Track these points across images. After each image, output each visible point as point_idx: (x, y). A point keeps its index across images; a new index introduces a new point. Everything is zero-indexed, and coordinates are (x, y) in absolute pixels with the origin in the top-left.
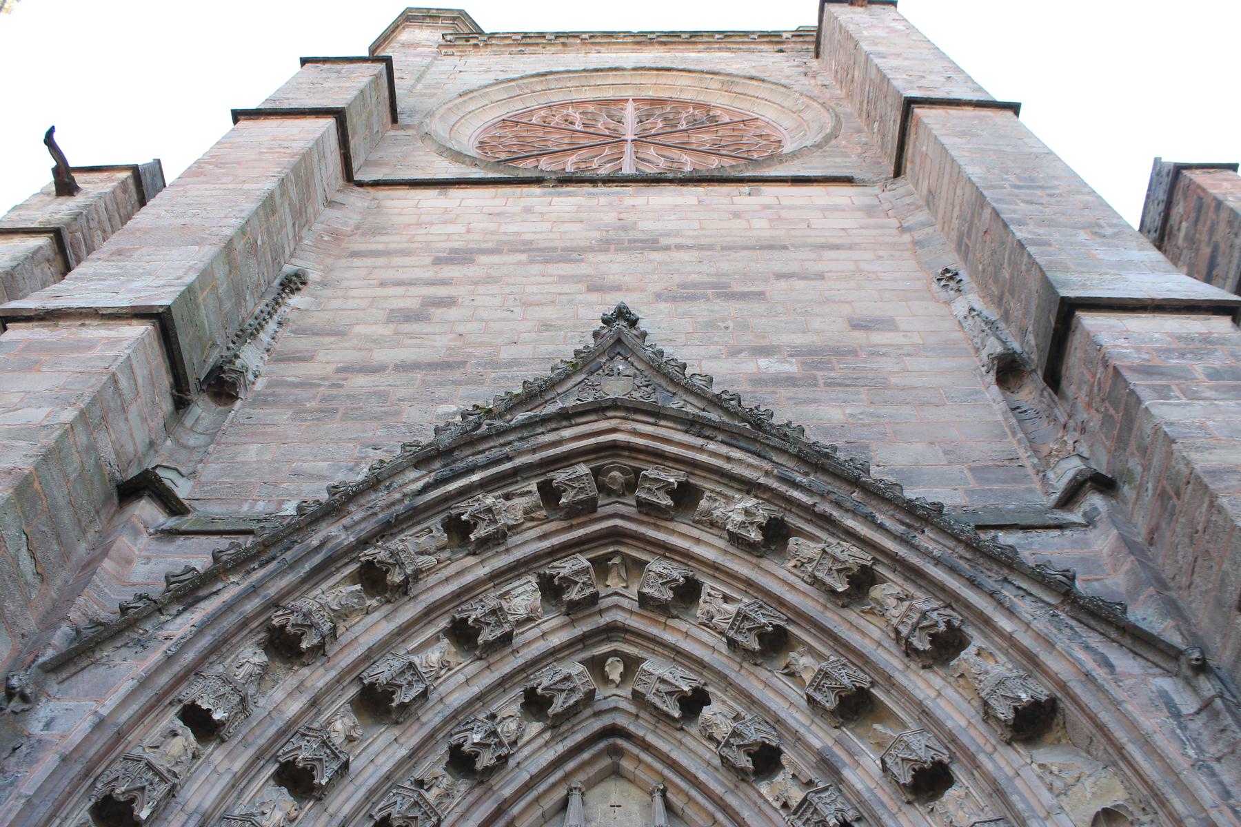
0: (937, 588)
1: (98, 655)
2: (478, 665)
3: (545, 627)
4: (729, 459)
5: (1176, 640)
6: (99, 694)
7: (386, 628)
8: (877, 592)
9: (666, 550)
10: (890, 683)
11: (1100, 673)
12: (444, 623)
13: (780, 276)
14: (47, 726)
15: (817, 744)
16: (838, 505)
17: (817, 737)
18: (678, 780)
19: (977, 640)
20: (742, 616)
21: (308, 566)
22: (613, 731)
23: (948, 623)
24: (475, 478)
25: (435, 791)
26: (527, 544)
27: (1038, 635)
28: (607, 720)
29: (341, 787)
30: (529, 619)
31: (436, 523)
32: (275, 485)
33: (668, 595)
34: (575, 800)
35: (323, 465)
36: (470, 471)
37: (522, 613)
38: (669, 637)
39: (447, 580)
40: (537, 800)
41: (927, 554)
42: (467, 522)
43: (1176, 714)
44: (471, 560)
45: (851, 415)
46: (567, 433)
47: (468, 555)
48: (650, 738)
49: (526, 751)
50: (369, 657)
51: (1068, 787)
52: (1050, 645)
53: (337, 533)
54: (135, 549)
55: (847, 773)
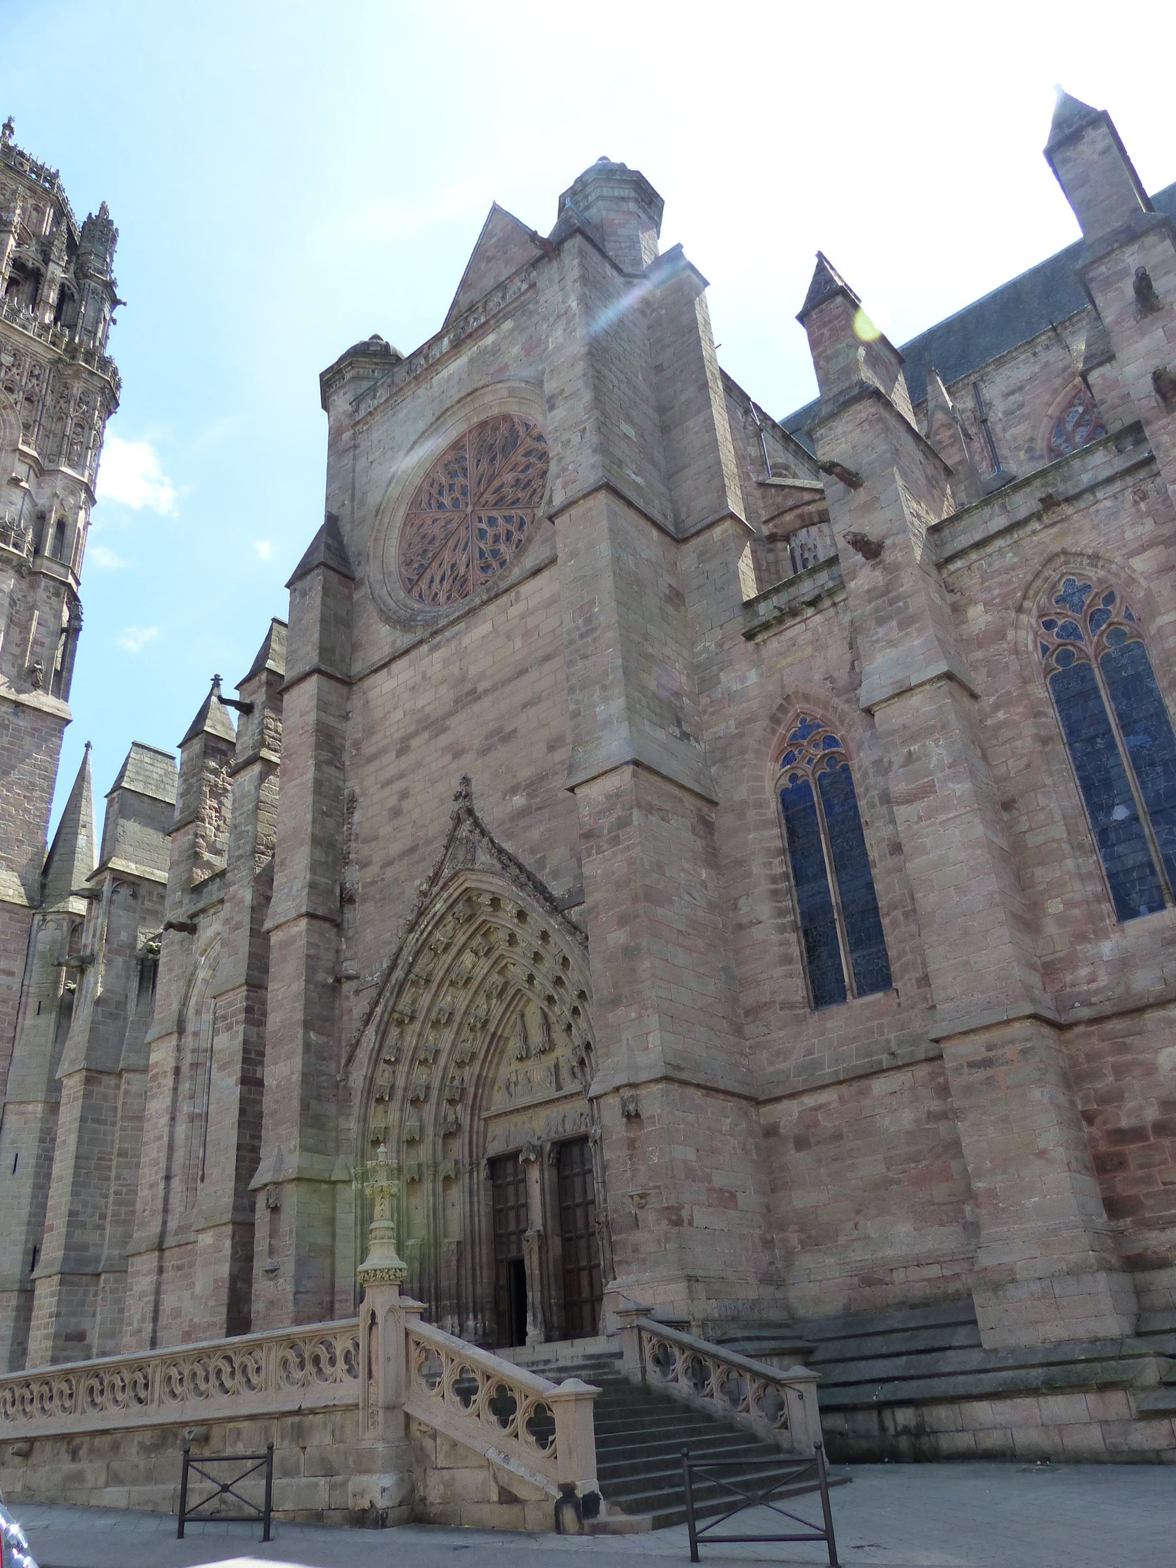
7: (430, 996)
12: (447, 984)
26: (461, 939)
31: (426, 950)
37: (470, 966)
44: (445, 957)
46: (451, 891)
50: (429, 1010)
53: (399, 974)
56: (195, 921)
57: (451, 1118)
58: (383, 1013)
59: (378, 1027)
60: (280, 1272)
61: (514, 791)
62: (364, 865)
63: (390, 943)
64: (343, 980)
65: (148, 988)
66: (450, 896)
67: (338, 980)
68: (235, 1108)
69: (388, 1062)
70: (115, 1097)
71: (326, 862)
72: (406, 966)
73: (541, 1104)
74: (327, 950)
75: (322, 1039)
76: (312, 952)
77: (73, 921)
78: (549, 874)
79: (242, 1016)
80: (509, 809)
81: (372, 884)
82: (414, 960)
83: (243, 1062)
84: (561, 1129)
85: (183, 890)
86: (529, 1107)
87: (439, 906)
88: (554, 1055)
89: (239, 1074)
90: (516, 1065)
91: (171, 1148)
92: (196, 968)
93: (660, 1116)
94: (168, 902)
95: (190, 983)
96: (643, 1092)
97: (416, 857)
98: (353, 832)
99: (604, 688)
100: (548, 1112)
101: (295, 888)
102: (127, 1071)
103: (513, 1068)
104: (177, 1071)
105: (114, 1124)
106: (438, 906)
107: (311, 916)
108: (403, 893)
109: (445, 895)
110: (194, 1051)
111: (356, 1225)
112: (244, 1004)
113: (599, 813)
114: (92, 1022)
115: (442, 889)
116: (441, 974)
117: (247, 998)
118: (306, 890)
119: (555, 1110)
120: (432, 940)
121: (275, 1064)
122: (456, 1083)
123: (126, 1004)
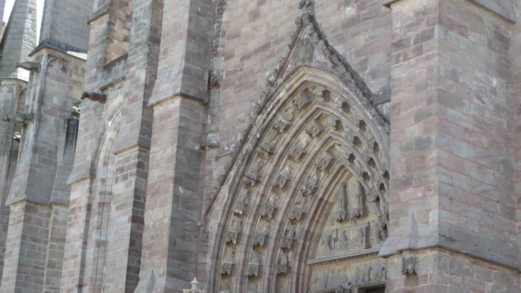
1: (213, 206)
2: (301, 164)
3: (314, 144)
12: (286, 157)
21: (245, 162)
24: (274, 112)
25: (301, 204)
26: (298, 122)
29: (278, 213)
30: (308, 145)
31: (271, 129)
32: (235, 128)
37: (305, 144)
39: (282, 144)
40: (332, 192)
42: (277, 128)
44: (285, 135)
45: (366, 40)
46: (292, 82)
47: (284, 134)
49: (322, 182)
50: (271, 177)
53: (248, 146)
54: (212, 167)
56: (106, 92)
57: (284, 262)
58: (235, 176)
59: (231, 186)
62: (229, 56)
63: (244, 121)
64: (207, 148)
65: (72, 142)
66: (291, 86)
67: (203, 148)
68: (127, 239)
69: (237, 214)
70: (47, 223)
71: (199, 53)
72: (255, 141)
73: (353, 257)
74: (196, 123)
75: (189, 193)
76: (183, 124)
77: (21, 87)
78: (369, 74)
79: (134, 170)
80: (342, 18)
81: (234, 72)
82: (261, 136)
83: (134, 205)
84: (367, 278)
85: (98, 68)
86: (345, 259)
87: (283, 94)
88: (367, 220)
89: (130, 214)
91: (83, 264)
92: (105, 129)
93: (431, 276)
94: (87, 76)
95: (100, 141)
96: (420, 256)
97: (268, 53)
98: (221, 29)
100: (358, 264)
101: (173, 73)
102: (57, 204)
103: (334, 227)
104: (89, 207)
105: (46, 243)
106: (281, 94)
107: (184, 95)
108: (256, 81)
109: (288, 86)
110: (101, 193)
112: (137, 160)
113: (408, 27)
114: (31, 165)
115: (285, 81)
116: (282, 148)
117: (139, 156)
118: (181, 75)
119: (364, 263)
120: (276, 121)
122: (289, 235)
123: (56, 153)
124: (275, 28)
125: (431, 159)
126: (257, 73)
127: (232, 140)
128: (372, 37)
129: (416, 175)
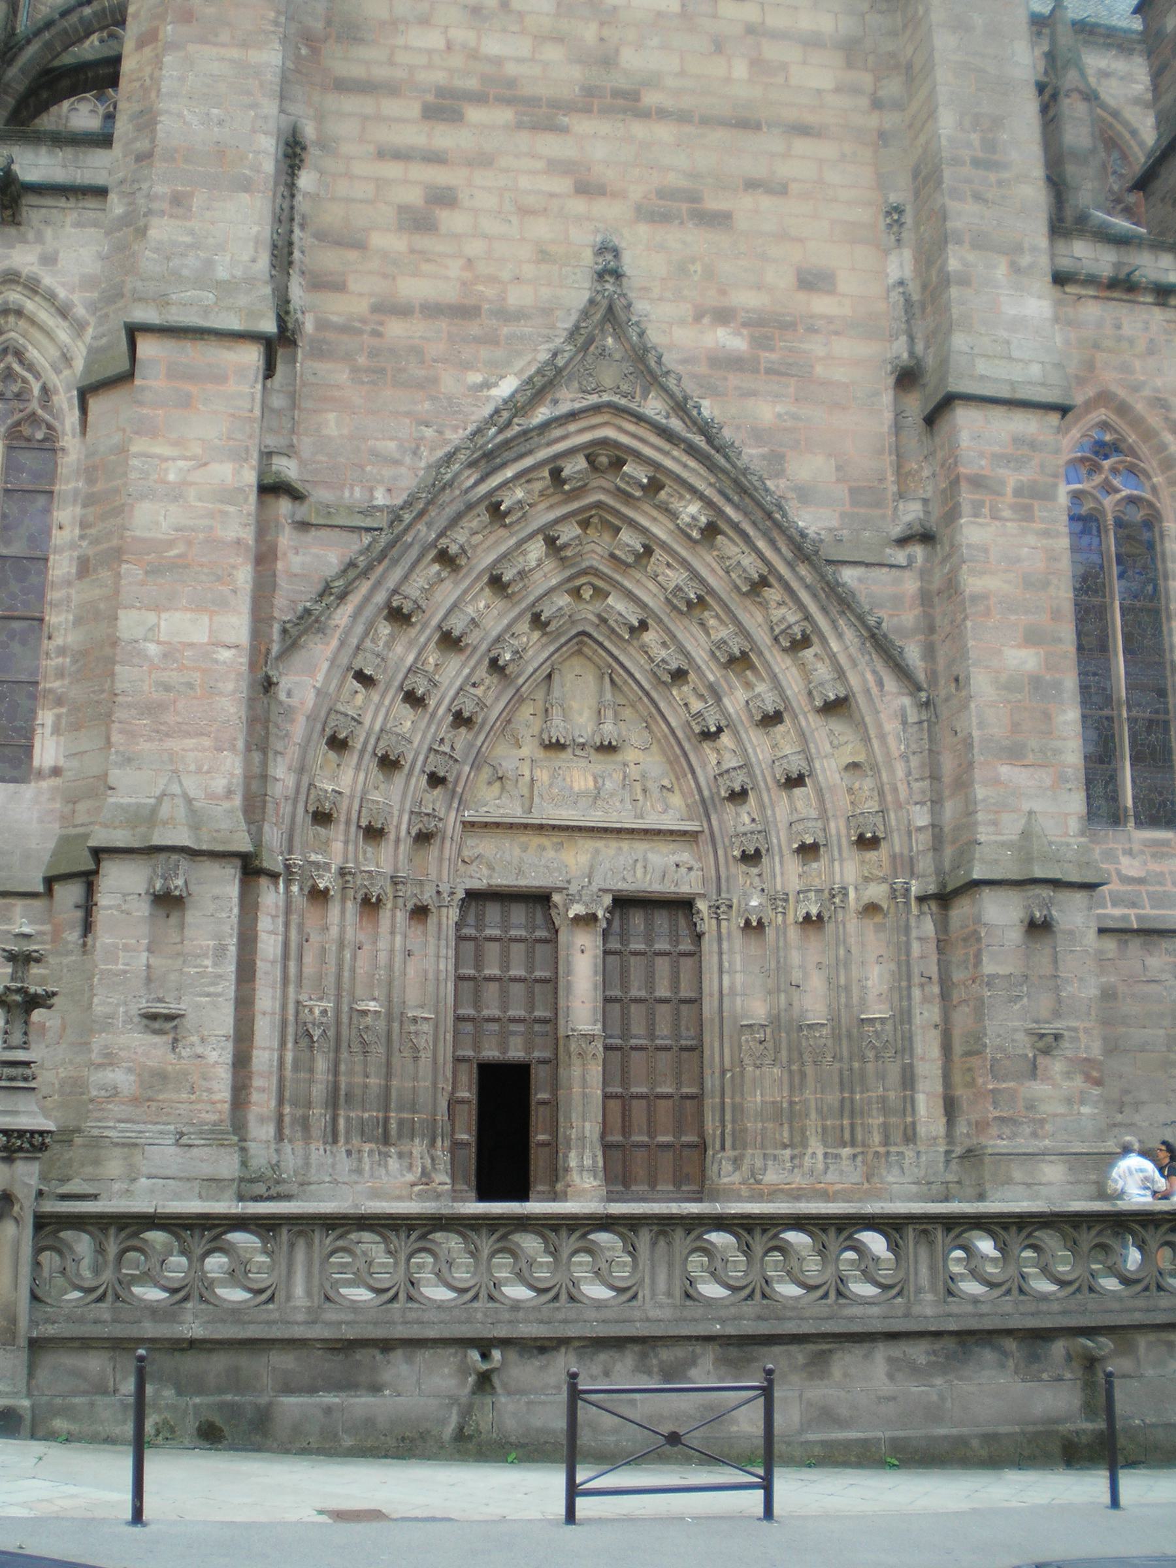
0: (802, 607)
4: (685, 466)
5: (921, 676)
6: (311, 670)
8: (768, 593)
9: (633, 524)
10: (760, 654)
11: (875, 690)
12: (485, 579)
13: (752, 185)
14: (289, 695)
15: (712, 678)
16: (754, 524)
17: (712, 672)
18: (621, 671)
19: (816, 648)
20: (678, 588)
22: (584, 633)
23: (803, 632)
24: (509, 473)
27: (850, 656)
28: (580, 629)
33: (630, 560)
34: (556, 677)
35: (391, 446)
36: (504, 465)
38: (627, 583)
41: (801, 579)
43: (904, 723)
44: (502, 532)
45: (779, 416)
46: (572, 427)
48: (607, 644)
51: (840, 745)
52: (855, 664)
55: (726, 701)
60: (189, 1022)
61: (723, 316)
62: (320, 283)
63: (396, 462)
88: (619, 757)
90: (529, 749)
99: (1015, 268)
100: (600, 844)
108: (435, 381)
111: (286, 956)
121: (157, 608)
124: (492, 279)
125: (1065, 723)
126: (435, 361)
127: (352, 494)
128: (796, 417)
129: (1033, 743)
